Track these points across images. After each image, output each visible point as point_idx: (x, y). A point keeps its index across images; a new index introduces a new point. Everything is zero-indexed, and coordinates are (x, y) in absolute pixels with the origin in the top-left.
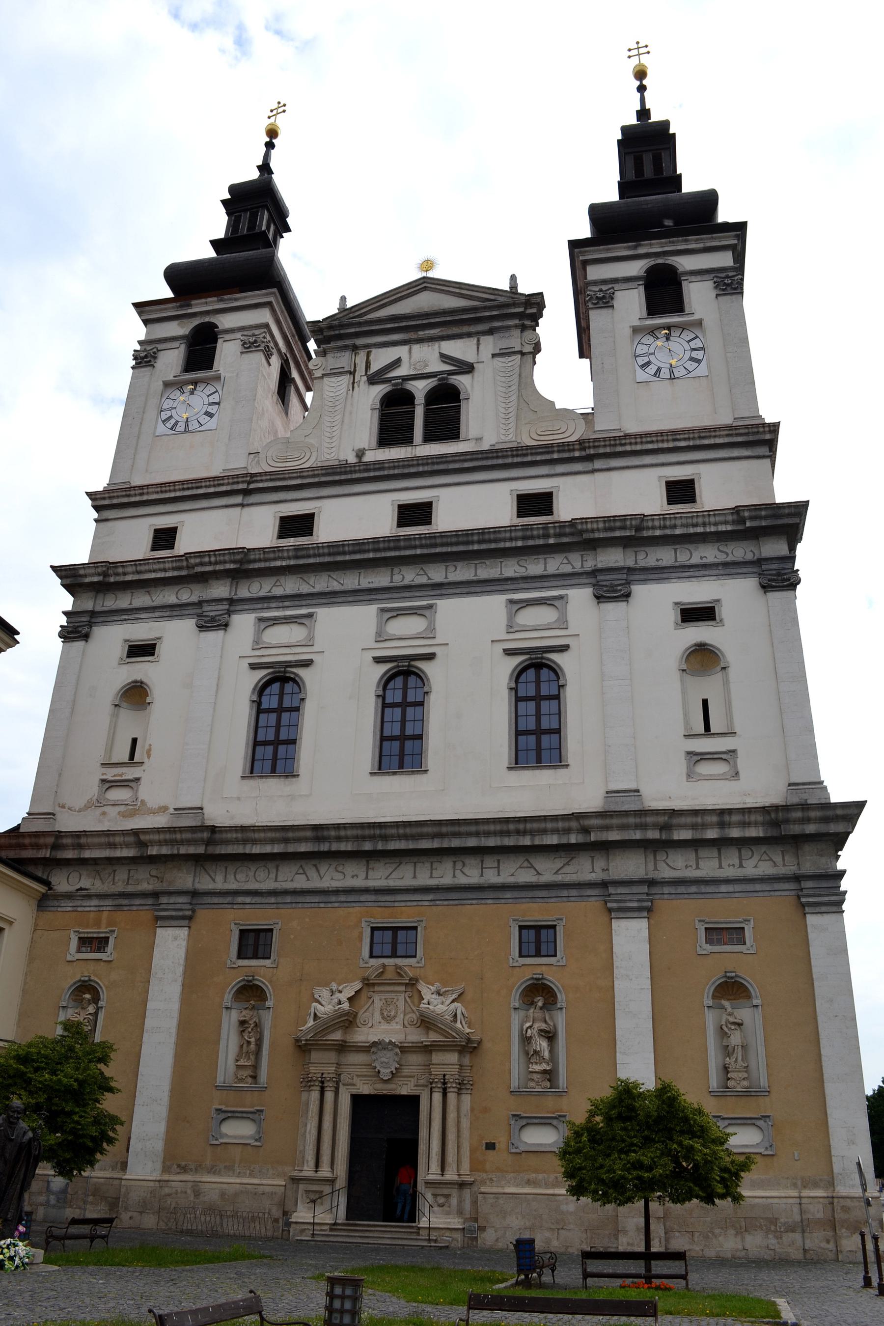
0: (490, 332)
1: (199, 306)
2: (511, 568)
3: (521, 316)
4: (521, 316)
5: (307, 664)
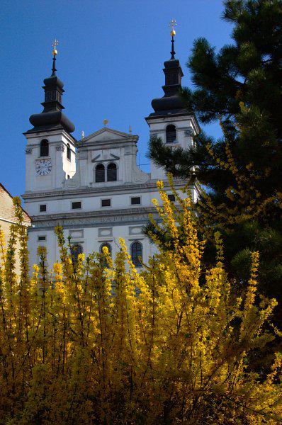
0: (123, 147)
1: (41, 134)
2: (130, 218)
3: (132, 142)
4: (132, 142)
5: (83, 242)
